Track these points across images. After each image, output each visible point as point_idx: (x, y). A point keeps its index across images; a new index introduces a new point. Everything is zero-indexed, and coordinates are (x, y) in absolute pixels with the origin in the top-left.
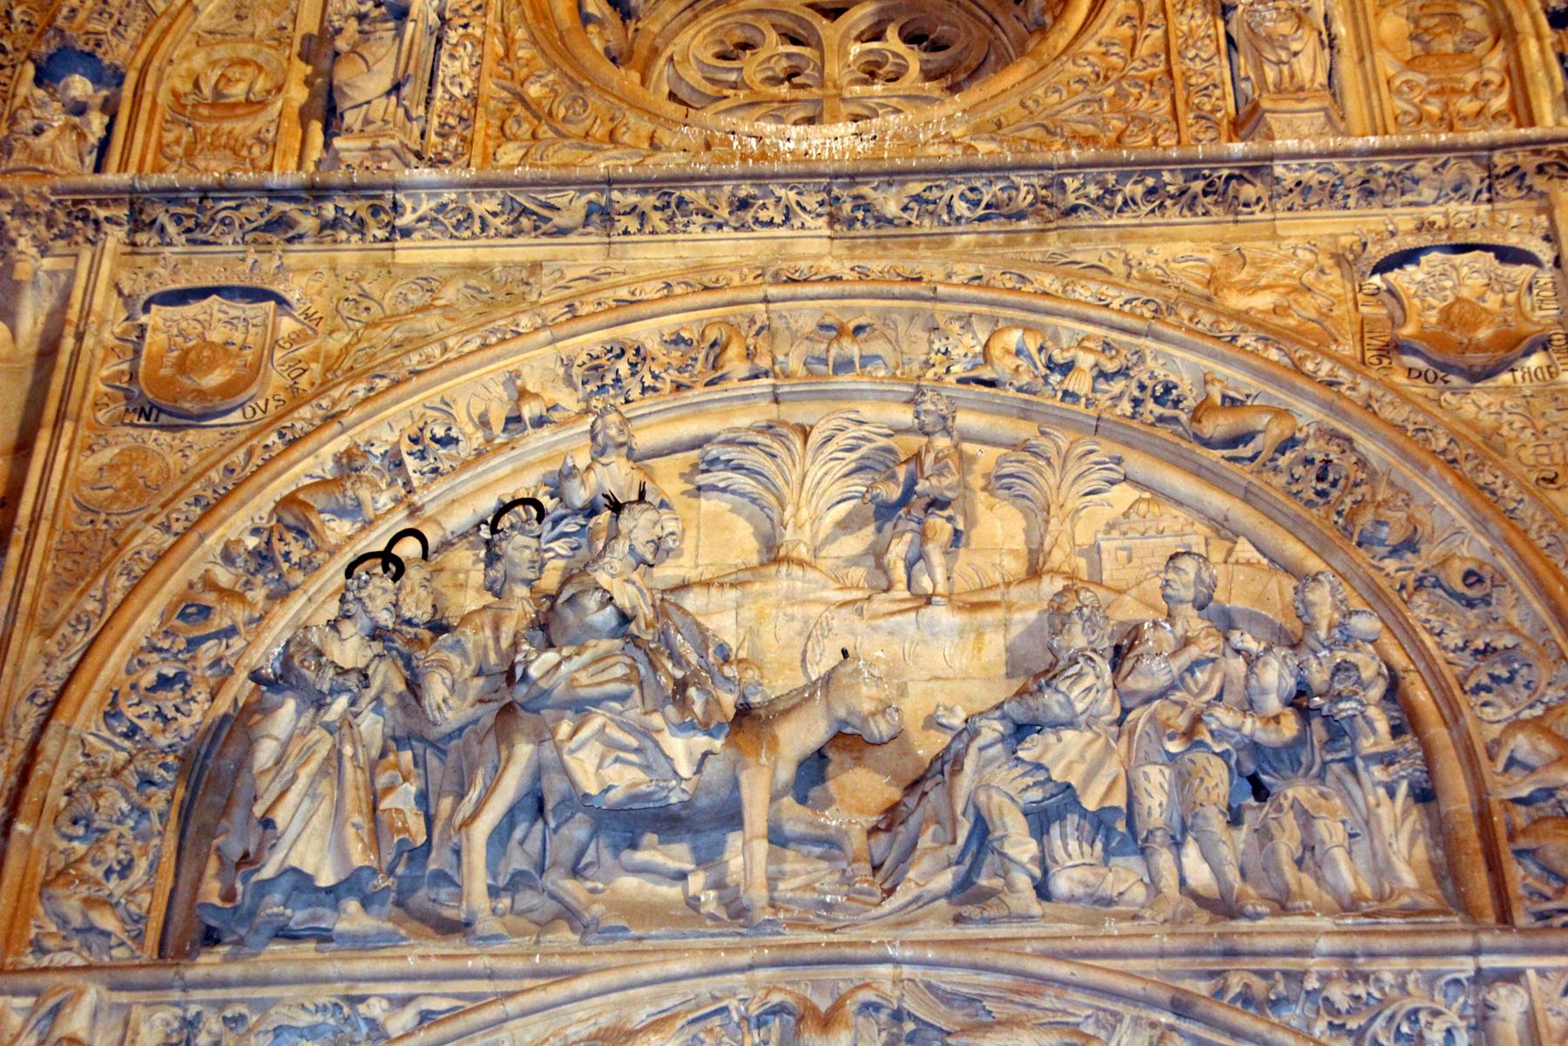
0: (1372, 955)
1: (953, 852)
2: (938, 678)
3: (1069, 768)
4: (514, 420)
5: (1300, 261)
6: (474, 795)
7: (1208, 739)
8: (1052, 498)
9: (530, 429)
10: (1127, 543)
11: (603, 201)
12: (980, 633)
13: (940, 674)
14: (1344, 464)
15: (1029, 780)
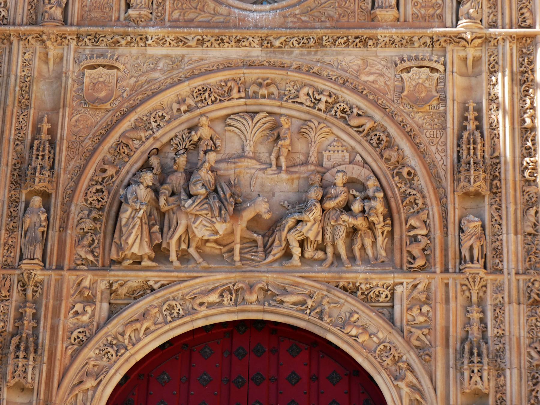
0: (371, 279)
1: (282, 248)
2: (282, 192)
3: (307, 232)
4: (179, 110)
5: (382, 65)
6: (172, 230)
7: (341, 222)
8: (313, 140)
9: (183, 114)
10: (330, 154)
11: (201, 39)
12: (293, 180)
13: (283, 190)
14: (383, 137)
15: (299, 234)
